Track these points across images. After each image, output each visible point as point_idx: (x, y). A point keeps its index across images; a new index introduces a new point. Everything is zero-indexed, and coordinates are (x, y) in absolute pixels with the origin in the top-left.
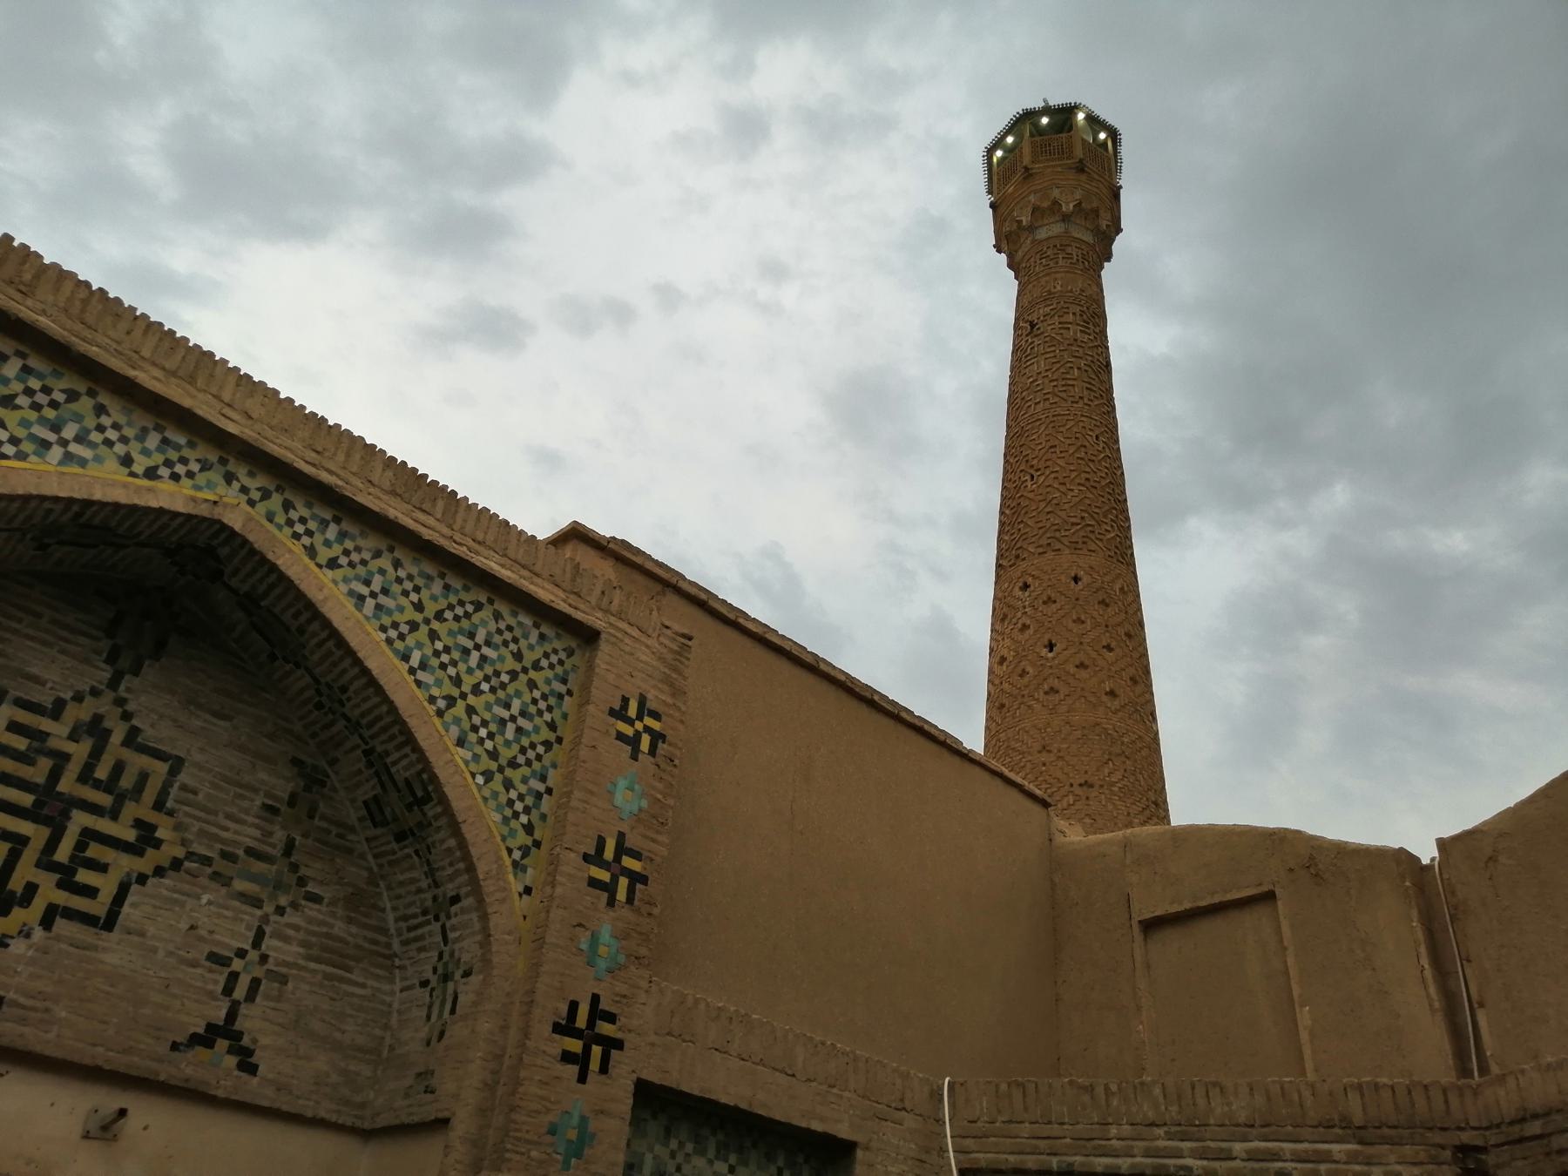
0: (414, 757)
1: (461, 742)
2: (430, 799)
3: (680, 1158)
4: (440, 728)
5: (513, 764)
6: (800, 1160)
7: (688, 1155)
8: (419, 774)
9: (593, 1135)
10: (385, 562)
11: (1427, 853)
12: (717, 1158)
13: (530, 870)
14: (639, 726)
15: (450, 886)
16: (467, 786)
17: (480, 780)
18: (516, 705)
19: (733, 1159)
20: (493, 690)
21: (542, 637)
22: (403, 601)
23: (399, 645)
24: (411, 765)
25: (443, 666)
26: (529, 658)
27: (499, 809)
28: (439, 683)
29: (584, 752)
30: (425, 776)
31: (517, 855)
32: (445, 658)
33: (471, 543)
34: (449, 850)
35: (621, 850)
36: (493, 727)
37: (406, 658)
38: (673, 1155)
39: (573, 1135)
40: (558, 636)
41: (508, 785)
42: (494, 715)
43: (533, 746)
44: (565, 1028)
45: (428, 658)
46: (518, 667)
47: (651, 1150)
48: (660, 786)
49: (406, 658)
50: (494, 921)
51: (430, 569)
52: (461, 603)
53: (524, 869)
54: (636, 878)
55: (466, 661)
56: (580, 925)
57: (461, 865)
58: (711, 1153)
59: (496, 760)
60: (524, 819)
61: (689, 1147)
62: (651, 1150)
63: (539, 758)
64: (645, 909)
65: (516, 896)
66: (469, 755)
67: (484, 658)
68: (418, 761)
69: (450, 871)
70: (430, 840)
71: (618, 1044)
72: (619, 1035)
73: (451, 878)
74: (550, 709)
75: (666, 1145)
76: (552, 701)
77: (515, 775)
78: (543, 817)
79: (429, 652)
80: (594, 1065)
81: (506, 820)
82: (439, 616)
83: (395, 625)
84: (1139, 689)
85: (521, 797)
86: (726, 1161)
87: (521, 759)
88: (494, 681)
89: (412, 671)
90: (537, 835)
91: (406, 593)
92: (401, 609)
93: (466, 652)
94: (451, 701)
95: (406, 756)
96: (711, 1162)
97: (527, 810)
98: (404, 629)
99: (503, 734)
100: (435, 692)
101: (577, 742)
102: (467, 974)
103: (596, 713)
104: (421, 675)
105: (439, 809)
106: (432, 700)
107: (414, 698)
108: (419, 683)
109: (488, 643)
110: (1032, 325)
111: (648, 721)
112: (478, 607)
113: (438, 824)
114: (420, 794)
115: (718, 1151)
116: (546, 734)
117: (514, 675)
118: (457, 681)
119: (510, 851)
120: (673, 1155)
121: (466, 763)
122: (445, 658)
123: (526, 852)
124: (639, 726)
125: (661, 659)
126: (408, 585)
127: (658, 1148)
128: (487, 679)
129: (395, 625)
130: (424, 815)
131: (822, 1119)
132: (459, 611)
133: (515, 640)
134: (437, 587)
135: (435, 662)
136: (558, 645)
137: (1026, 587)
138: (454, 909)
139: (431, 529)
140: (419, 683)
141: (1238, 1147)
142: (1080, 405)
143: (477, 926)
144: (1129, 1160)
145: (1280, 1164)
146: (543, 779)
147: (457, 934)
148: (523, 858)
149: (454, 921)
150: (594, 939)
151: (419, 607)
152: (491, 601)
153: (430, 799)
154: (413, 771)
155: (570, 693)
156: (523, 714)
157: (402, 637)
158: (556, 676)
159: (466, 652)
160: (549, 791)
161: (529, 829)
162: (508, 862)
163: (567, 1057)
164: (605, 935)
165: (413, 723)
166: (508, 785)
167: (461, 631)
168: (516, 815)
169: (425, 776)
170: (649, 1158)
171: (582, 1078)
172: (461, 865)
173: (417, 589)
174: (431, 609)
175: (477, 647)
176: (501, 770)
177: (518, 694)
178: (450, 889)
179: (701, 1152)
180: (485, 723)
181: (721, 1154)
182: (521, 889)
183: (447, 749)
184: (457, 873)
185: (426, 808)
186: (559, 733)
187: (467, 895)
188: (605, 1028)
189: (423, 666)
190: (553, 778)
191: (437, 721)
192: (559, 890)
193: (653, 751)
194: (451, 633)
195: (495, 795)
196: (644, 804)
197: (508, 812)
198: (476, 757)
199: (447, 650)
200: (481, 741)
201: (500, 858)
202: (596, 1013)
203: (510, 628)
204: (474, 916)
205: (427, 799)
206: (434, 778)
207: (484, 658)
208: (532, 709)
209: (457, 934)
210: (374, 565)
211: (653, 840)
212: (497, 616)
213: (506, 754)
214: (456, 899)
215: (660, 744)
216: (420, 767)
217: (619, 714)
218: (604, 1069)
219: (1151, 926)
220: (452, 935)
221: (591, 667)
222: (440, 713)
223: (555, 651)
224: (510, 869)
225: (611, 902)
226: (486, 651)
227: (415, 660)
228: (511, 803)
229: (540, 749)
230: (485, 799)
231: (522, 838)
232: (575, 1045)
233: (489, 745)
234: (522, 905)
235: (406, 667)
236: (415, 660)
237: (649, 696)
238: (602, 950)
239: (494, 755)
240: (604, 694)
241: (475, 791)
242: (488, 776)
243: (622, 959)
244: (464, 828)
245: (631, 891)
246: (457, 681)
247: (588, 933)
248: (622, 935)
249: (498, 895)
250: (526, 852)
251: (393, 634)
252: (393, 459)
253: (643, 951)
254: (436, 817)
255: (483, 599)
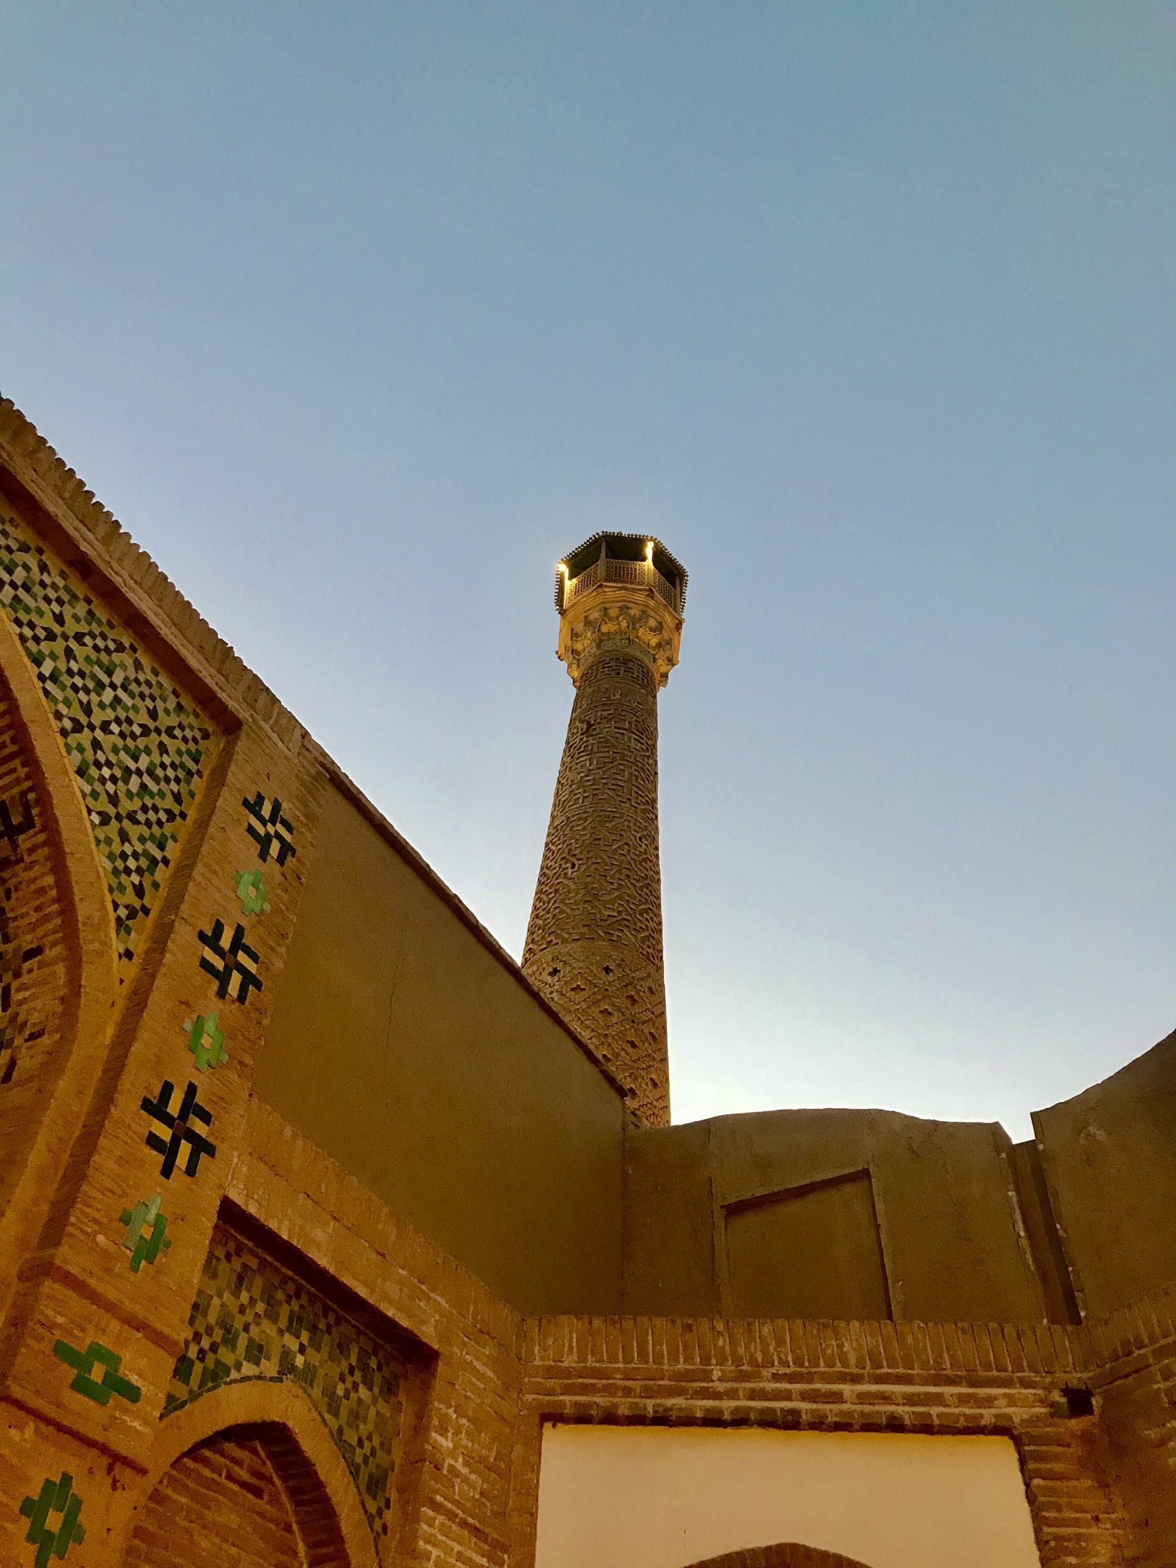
0: (22, 772)
1: (81, 772)
2: (31, 825)
3: (249, 1317)
4: (63, 750)
5: (132, 817)
6: (373, 1363)
7: (257, 1315)
8: (23, 794)
9: (168, 1244)
10: (31, 560)
11: (1021, 1132)
12: (289, 1329)
13: (133, 933)
14: (271, 829)
15: (29, 938)
16: (80, 818)
17: (96, 819)
18: (144, 762)
19: (305, 1337)
20: (122, 735)
21: (180, 707)
22: (44, 606)
23: (31, 644)
24: (18, 781)
25: (75, 688)
26: (165, 721)
27: (111, 857)
28: (67, 702)
29: (212, 830)
30: (31, 796)
31: (122, 912)
32: (78, 681)
33: (127, 578)
34: (42, 891)
35: (237, 943)
36: (118, 773)
37: (37, 661)
38: (242, 1310)
39: (147, 1232)
40: (196, 715)
41: (124, 837)
42: (119, 761)
43: (155, 809)
44: (155, 1108)
45: (61, 674)
46: (151, 724)
47: (220, 1295)
48: (285, 896)
49: (37, 661)
50: (87, 972)
51: (80, 589)
52: (104, 637)
53: (128, 931)
54: (249, 979)
55: (99, 695)
56: (187, 1004)
57: (55, 907)
58: (283, 1322)
59: (116, 806)
60: (135, 878)
61: (260, 1307)
62: (220, 1295)
63: (160, 823)
64: (254, 1016)
65: (116, 957)
66: (88, 789)
67: (117, 700)
68: (28, 777)
69: (34, 917)
70: (11, 884)
71: (210, 1150)
72: (211, 1140)
73: (33, 927)
74: (177, 780)
75: (236, 1294)
76: (181, 774)
77: (134, 831)
78: (156, 885)
79: (63, 667)
80: (182, 1160)
81: (116, 872)
82: (79, 637)
83: (31, 625)
84: (658, 1093)
85: (135, 855)
86: (298, 1337)
87: (141, 817)
88: (125, 726)
89: (41, 677)
90: (147, 901)
91: (48, 600)
92: (41, 613)
93: (100, 686)
94: (78, 727)
95: (13, 771)
96: (281, 1332)
97: (140, 871)
98: (42, 634)
99: (126, 782)
100: (64, 710)
101: (203, 824)
102: (33, 1037)
103: (228, 803)
104: (49, 685)
105: (41, 837)
106: (58, 716)
107: (39, 705)
108: (46, 693)
109: (124, 687)
110: (589, 725)
111: (279, 827)
112: (120, 648)
113: (34, 857)
114: (16, 820)
115: (290, 1321)
116: (169, 803)
117: (146, 731)
118: (87, 709)
119: (116, 906)
120: (242, 1310)
121: (84, 796)
122: (78, 681)
123: (132, 915)
124: (271, 829)
125: (301, 780)
126: (52, 595)
127: (227, 1296)
128: (118, 721)
129: (31, 625)
130: (15, 846)
131: (409, 1315)
132: (101, 643)
133: (153, 698)
134: (81, 609)
135: (66, 680)
136: (192, 720)
137: (555, 972)
138: (26, 966)
139: (90, 545)
140: (46, 693)
141: (847, 1389)
142: (627, 805)
143: (62, 979)
144: (734, 1403)
145: (893, 1408)
146: (161, 847)
147: (20, 996)
148: (128, 918)
149: (25, 978)
150: (199, 1022)
151: (59, 619)
152: (133, 649)
153: (31, 825)
154: (16, 791)
155: (199, 773)
156: (150, 772)
157: (36, 639)
158: (188, 752)
159: (100, 686)
160: (166, 861)
161: (139, 891)
162: (112, 916)
163: (153, 1141)
164: (210, 1026)
165: (33, 730)
166: (124, 837)
167: (99, 663)
168: (128, 871)
169: (31, 796)
170: (216, 1302)
171: (167, 1171)
172: (55, 907)
173: (60, 602)
174: (71, 627)
175: (113, 686)
176: (119, 817)
177: (148, 752)
178: (27, 941)
179: (274, 1319)
180: (109, 764)
181: (295, 1323)
182: (122, 951)
183: (66, 772)
184: (47, 918)
185: (22, 837)
186: (183, 808)
187: (53, 945)
188: (199, 1127)
189: (54, 678)
190: (173, 851)
191: (59, 738)
192: (168, 958)
193: (281, 860)
194: (87, 659)
195: (109, 841)
196: (267, 907)
197: (120, 864)
198: (95, 795)
199: (82, 674)
200: (103, 780)
201: (104, 907)
202: (189, 1105)
203: (149, 684)
204: (60, 969)
205: (28, 823)
206: (45, 800)
207: (117, 700)
208: (160, 772)
209: (20, 996)
210: (20, 557)
211: (272, 949)
212: (138, 666)
213: (127, 805)
214: (37, 951)
215: (289, 858)
216: (28, 784)
217: (253, 807)
218: (191, 1170)
219: (735, 1210)
220: (16, 997)
221: (227, 755)
222: (64, 733)
223: (192, 728)
224: (113, 924)
225: (222, 993)
226: (120, 693)
227: (47, 668)
228: (124, 856)
229: (163, 817)
230: (98, 842)
231: (130, 898)
232: (165, 1133)
233: (110, 787)
234: (119, 967)
235: (36, 670)
236: (47, 668)
237: (284, 805)
238: (206, 1041)
239: (114, 800)
240: (241, 778)
241: (90, 830)
242: (105, 819)
243: (225, 1058)
244: (70, 863)
245: (243, 989)
246: (87, 709)
247: (194, 1016)
248: (228, 1033)
249: (96, 946)
250: (132, 915)
251: (28, 632)
252: (60, 462)
253: (248, 1059)
254: (31, 851)
255: (127, 645)
